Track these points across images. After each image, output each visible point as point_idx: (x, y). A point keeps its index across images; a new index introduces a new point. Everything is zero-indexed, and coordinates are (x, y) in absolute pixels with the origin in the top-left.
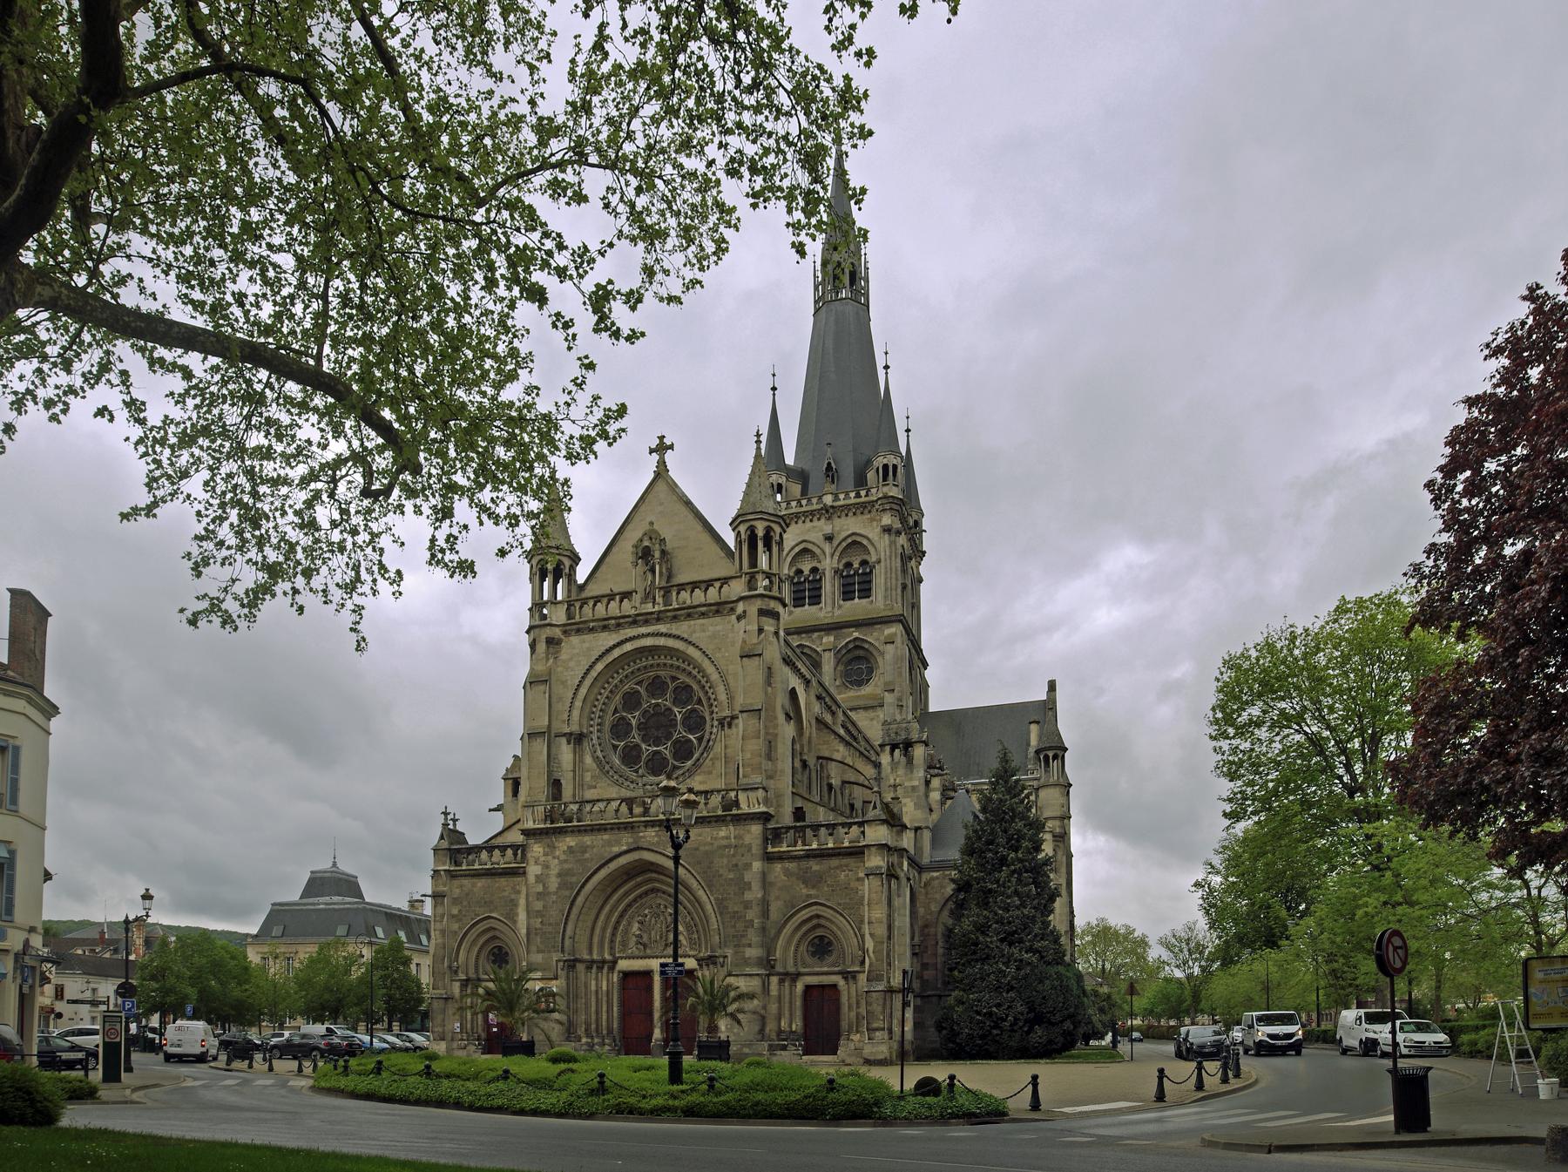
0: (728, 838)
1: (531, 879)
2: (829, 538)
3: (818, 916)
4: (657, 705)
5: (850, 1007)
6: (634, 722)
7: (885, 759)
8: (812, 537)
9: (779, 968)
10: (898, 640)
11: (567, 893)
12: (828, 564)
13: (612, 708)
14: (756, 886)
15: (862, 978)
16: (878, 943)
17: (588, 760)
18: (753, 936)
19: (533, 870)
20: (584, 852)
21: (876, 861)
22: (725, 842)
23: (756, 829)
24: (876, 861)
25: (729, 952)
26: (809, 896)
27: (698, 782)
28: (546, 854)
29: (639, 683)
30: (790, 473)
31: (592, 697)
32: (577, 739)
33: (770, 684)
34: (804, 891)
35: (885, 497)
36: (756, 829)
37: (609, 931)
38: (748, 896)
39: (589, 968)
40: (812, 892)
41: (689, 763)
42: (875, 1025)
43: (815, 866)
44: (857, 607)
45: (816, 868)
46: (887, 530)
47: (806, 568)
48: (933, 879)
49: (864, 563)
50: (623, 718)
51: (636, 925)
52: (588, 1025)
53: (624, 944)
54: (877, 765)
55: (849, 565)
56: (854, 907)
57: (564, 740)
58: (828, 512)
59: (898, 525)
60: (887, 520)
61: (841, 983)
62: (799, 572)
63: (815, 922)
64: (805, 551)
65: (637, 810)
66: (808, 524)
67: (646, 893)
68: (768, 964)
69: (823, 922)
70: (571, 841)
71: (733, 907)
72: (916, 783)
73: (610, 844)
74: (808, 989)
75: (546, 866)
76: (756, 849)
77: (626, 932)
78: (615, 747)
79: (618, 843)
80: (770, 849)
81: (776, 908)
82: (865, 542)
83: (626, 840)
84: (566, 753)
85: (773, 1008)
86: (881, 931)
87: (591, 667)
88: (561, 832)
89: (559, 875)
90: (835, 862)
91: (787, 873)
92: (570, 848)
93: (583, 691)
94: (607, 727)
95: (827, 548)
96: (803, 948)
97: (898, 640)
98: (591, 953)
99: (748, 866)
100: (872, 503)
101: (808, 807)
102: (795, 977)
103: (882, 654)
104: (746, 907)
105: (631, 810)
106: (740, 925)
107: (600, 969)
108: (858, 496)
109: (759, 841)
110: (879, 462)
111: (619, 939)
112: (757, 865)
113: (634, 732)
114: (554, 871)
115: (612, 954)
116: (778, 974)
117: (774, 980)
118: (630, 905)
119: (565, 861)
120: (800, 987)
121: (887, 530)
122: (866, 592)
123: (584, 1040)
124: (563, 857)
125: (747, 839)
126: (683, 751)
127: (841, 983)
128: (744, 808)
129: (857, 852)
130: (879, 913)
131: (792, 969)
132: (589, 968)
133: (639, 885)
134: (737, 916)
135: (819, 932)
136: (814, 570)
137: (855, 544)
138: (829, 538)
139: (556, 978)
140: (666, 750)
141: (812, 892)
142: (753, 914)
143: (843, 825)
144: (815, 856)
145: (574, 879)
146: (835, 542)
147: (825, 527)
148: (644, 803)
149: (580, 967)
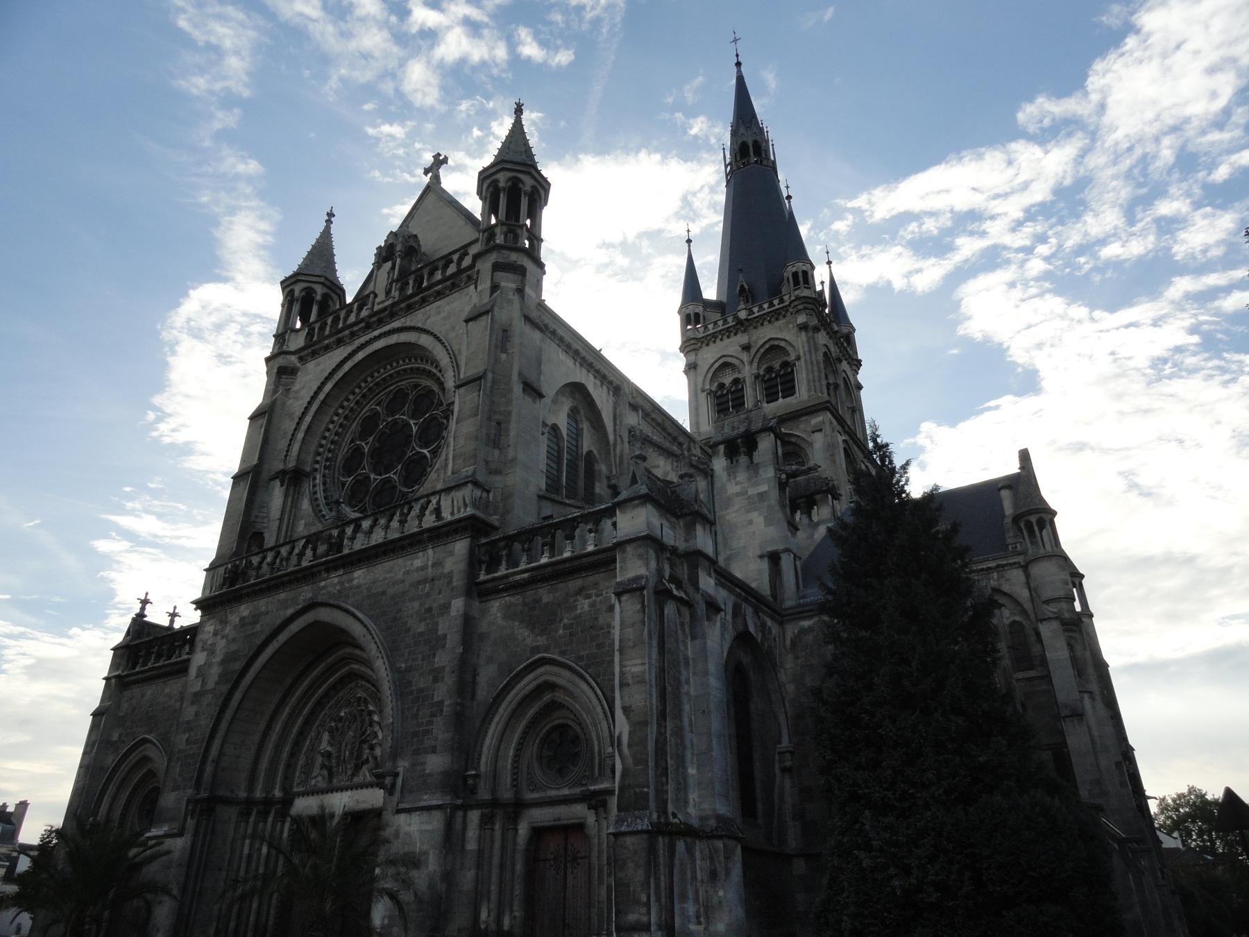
0: (423, 568)
1: (193, 671)
2: (746, 348)
3: (552, 686)
5: (600, 871)
8: (730, 351)
9: (484, 794)
10: (827, 428)
12: (747, 372)
13: (348, 438)
14: (453, 640)
15: (613, 802)
16: (638, 726)
17: (305, 504)
18: (441, 732)
20: (255, 623)
21: (633, 567)
22: (416, 577)
23: (461, 547)
24: (633, 567)
25: (403, 765)
26: (536, 649)
28: (215, 634)
29: (378, 404)
30: (708, 304)
32: (294, 478)
33: (504, 350)
35: (798, 298)
36: (461, 547)
37: (287, 749)
39: (245, 814)
40: (542, 641)
42: (632, 917)
43: (545, 595)
44: (782, 404)
46: (803, 327)
47: (727, 380)
48: (803, 631)
49: (785, 364)
51: (326, 736)
55: (769, 370)
56: (597, 667)
57: (278, 483)
58: (742, 326)
59: (814, 322)
60: (801, 319)
61: (591, 819)
62: (722, 386)
63: (547, 697)
64: (726, 365)
66: (726, 341)
67: (342, 681)
68: (460, 787)
69: (559, 696)
70: (245, 610)
72: (764, 488)
73: (284, 604)
74: (538, 833)
75: (212, 652)
76: (458, 582)
80: (483, 577)
81: (487, 676)
82: (783, 344)
83: (305, 593)
84: (277, 497)
85: (467, 878)
86: (641, 698)
87: (320, 389)
89: (223, 662)
90: (575, 584)
93: (308, 419)
95: (745, 357)
96: (531, 751)
97: (827, 428)
98: (251, 789)
99: (446, 607)
100: (786, 308)
102: (517, 807)
103: (811, 444)
104: (436, 680)
105: (314, 549)
107: (264, 815)
108: (771, 305)
109: (462, 566)
110: (790, 270)
111: (301, 762)
112: (458, 605)
114: (217, 659)
116: (480, 805)
117: (474, 816)
118: (320, 704)
119: (234, 640)
120: (523, 830)
121: (803, 327)
122: (789, 390)
127: (591, 819)
129: (604, 561)
130: (637, 664)
131: (507, 794)
132: (245, 814)
133: (330, 670)
135: (557, 719)
136: (736, 381)
137: (774, 349)
138: (746, 348)
139: (180, 834)
141: (542, 641)
142: (443, 691)
143: (585, 518)
144: (545, 579)
146: (753, 351)
147: (742, 339)
149: (230, 814)
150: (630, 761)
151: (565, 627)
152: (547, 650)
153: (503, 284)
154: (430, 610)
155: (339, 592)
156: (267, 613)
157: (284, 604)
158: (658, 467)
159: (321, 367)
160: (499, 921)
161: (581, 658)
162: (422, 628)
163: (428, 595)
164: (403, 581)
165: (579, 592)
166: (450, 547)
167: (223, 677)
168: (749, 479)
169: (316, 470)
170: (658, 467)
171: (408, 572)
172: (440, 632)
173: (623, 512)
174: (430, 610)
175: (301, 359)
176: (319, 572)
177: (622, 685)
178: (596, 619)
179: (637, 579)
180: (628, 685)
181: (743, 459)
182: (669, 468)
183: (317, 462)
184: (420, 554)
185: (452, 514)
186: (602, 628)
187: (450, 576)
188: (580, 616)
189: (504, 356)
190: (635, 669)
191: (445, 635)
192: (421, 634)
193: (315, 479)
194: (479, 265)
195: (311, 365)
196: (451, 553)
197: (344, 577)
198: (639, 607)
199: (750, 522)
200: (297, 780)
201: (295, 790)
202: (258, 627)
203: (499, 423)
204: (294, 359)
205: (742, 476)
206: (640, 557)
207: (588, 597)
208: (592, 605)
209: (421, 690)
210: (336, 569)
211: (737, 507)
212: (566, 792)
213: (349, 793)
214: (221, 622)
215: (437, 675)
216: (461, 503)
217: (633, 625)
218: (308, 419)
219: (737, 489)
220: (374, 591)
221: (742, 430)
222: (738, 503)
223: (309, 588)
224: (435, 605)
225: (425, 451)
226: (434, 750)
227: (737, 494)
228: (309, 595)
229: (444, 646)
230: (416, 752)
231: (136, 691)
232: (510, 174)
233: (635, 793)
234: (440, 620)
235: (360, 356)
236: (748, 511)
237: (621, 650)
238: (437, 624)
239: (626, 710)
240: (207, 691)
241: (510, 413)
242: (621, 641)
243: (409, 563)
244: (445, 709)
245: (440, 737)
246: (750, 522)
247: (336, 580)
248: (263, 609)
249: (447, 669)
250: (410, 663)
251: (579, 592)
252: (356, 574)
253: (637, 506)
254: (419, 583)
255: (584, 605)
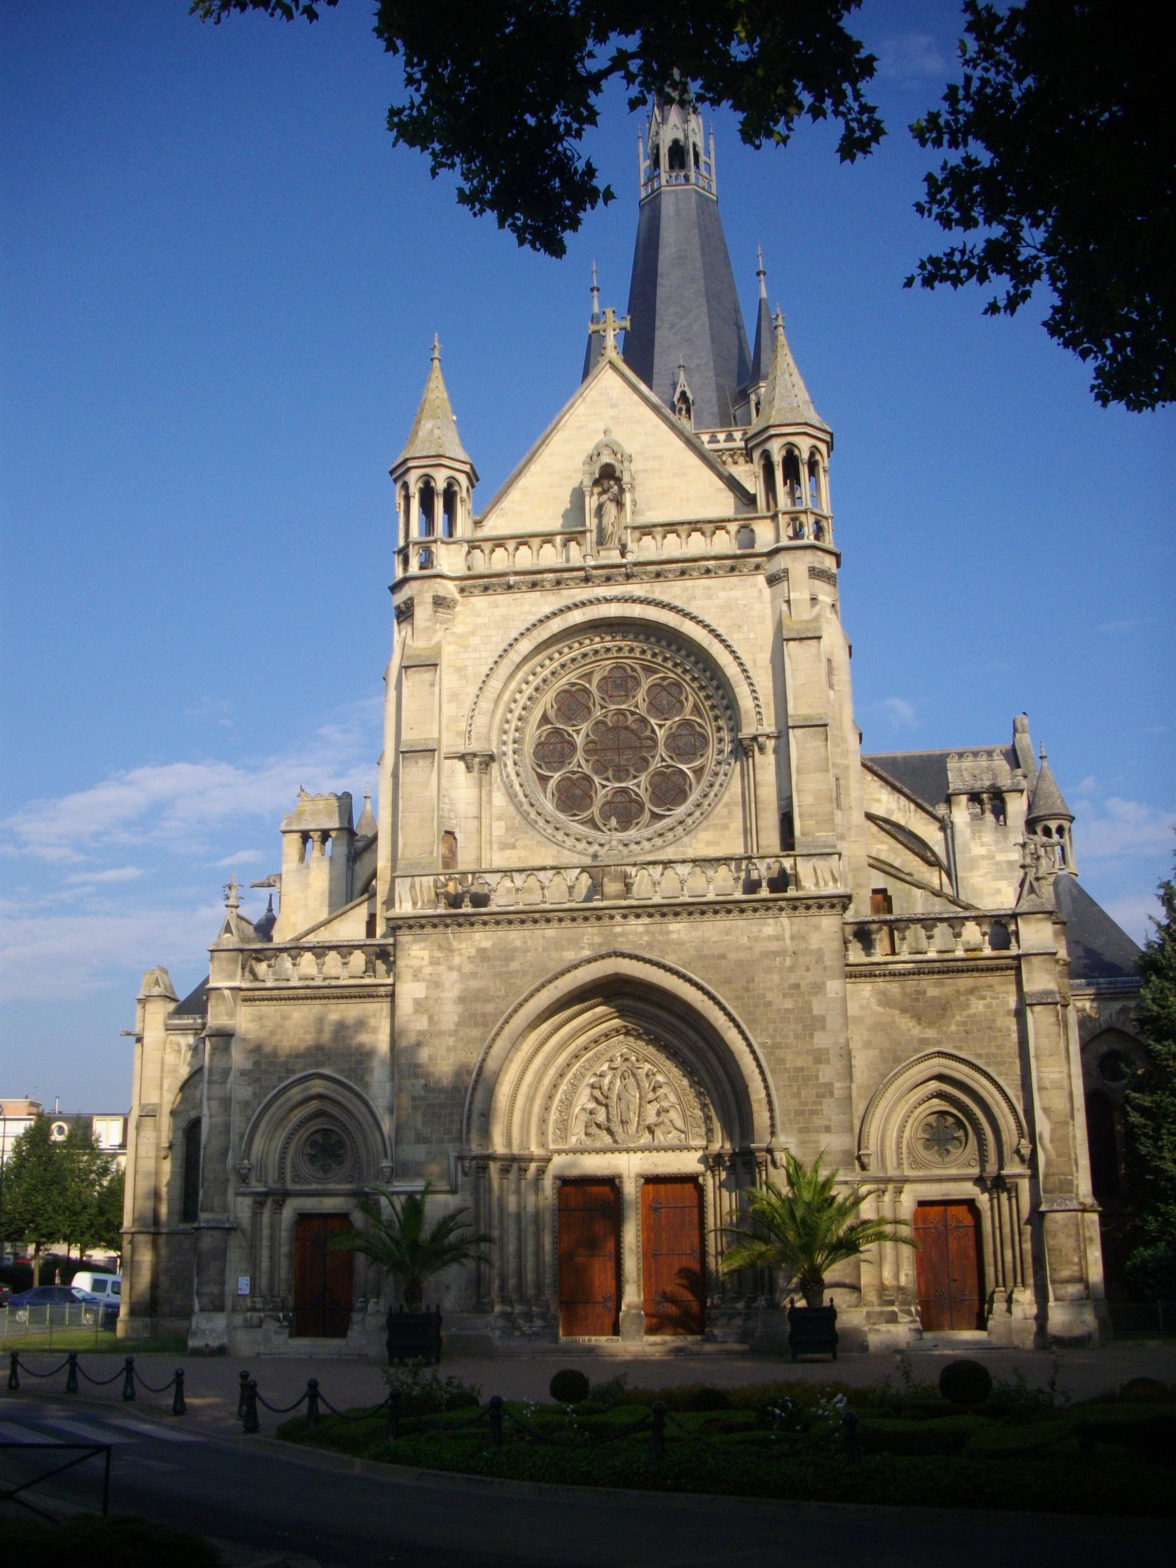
0: (779, 938)
4: (620, 712)
6: (579, 740)
7: (961, 814)
9: (874, 1170)
11: (476, 1032)
13: (537, 714)
17: (499, 799)
18: (830, 1111)
19: (410, 991)
20: (509, 958)
22: (774, 946)
23: (829, 923)
26: (924, 1042)
27: (702, 844)
28: (434, 962)
31: (507, 695)
32: (481, 762)
33: (831, 686)
34: (916, 1031)
37: (538, 1102)
38: (821, 1040)
41: (680, 811)
43: (931, 988)
45: (932, 992)
50: (557, 731)
52: (503, 1279)
53: (564, 1128)
54: (945, 826)
65: (612, 887)
70: (482, 938)
71: (793, 1061)
73: (558, 946)
76: (831, 959)
77: (568, 1103)
78: (543, 779)
79: (574, 943)
88: (468, 921)
89: (461, 1000)
90: (965, 982)
91: (886, 1001)
92: (482, 952)
93: (495, 684)
94: (529, 747)
99: (818, 988)
101: (894, 888)
104: (818, 1060)
106: (809, 1093)
109: (837, 945)
111: (553, 1116)
113: (579, 756)
115: (543, 1145)
116: (877, 1180)
119: (474, 975)
123: (498, 1308)
124: (468, 968)
125: (815, 942)
126: (671, 791)
128: (809, 886)
131: (892, 1172)
134: (801, 1077)
140: (640, 785)
141: (930, 1033)
145: (490, 1008)
148: (626, 876)
150: (1053, 1153)
151: (958, 1024)
152: (939, 1042)
153: (821, 597)
154: (797, 986)
155: (650, 945)
156: (527, 951)
157: (558, 946)
158: (879, 801)
159: (499, 612)
160: (897, 1276)
161: (979, 1056)
162: (789, 1004)
163: (792, 969)
164: (750, 948)
165: (972, 991)
166: (815, 920)
167: (470, 1018)
168: (997, 842)
169: (505, 754)
170: (879, 801)
171: (757, 939)
172: (815, 1012)
173: (1026, 922)
174: (797, 986)
175: (462, 590)
176: (612, 917)
177: (1040, 1089)
178: (994, 1020)
179: (1048, 993)
180: (1046, 1089)
181: (989, 817)
182: (894, 806)
183: (505, 743)
184: (771, 921)
185: (817, 884)
186: (1000, 1031)
187: (819, 956)
188: (974, 1015)
189: (832, 693)
190: (1052, 1076)
191: (823, 1019)
192: (787, 1011)
193: (506, 765)
194: (782, 561)
195: (480, 602)
196: (817, 928)
197: (653, 928)
198: (1053, 1019)
199: (998, 891)
200: (550, 1137)
201: (552, 1147)
202: (514, 966)
203: (837, 779)
204: (450, 585)
205: (988, 837)
206: (1048, 971)
207: (983, 998)
208: (989, 1006)
209: (801, 1069)
210: (638, 916)
211: (983, 871)
212: (953, 1171)
213: (639, 1154)
214: (440, 947)
215: (820, 1057)
216: (828, 877)
217: (1048, 1036)
218: (495, 684)
219: (983, 851)
220: (706, 952)
221: (987, 783)
222: (985, 867)
223: (596, 930)
224: (803, 983)
225: (683, 767)
226: (828, 1129)
227: (983, 857)
228: (598, 940)
229: (824, 1028)
230: (805, 1130)
231: (268, 1009)
232: (813, 442)
233: (1060, 1180)
234: (813, 999)
235: (577, 617)
236: (995, 879)
237: (1037, 1057)
238: (809, 1003)
239: (1046, 1110)
240: (441, 1033)
241: (847, 767)
242: (1036, 1048)
243: (755, 929)
244: (836, 1092)
245: (834, 1117)
246: (998, 891)
247: (641, 929)
248: (518, 943)
249: (831, 1052)
250: (778, 1040)
251: (972, 991)
252: (674, 927)
253: (1042, 920)
254: (777, 954)
255: (978, 1006)
